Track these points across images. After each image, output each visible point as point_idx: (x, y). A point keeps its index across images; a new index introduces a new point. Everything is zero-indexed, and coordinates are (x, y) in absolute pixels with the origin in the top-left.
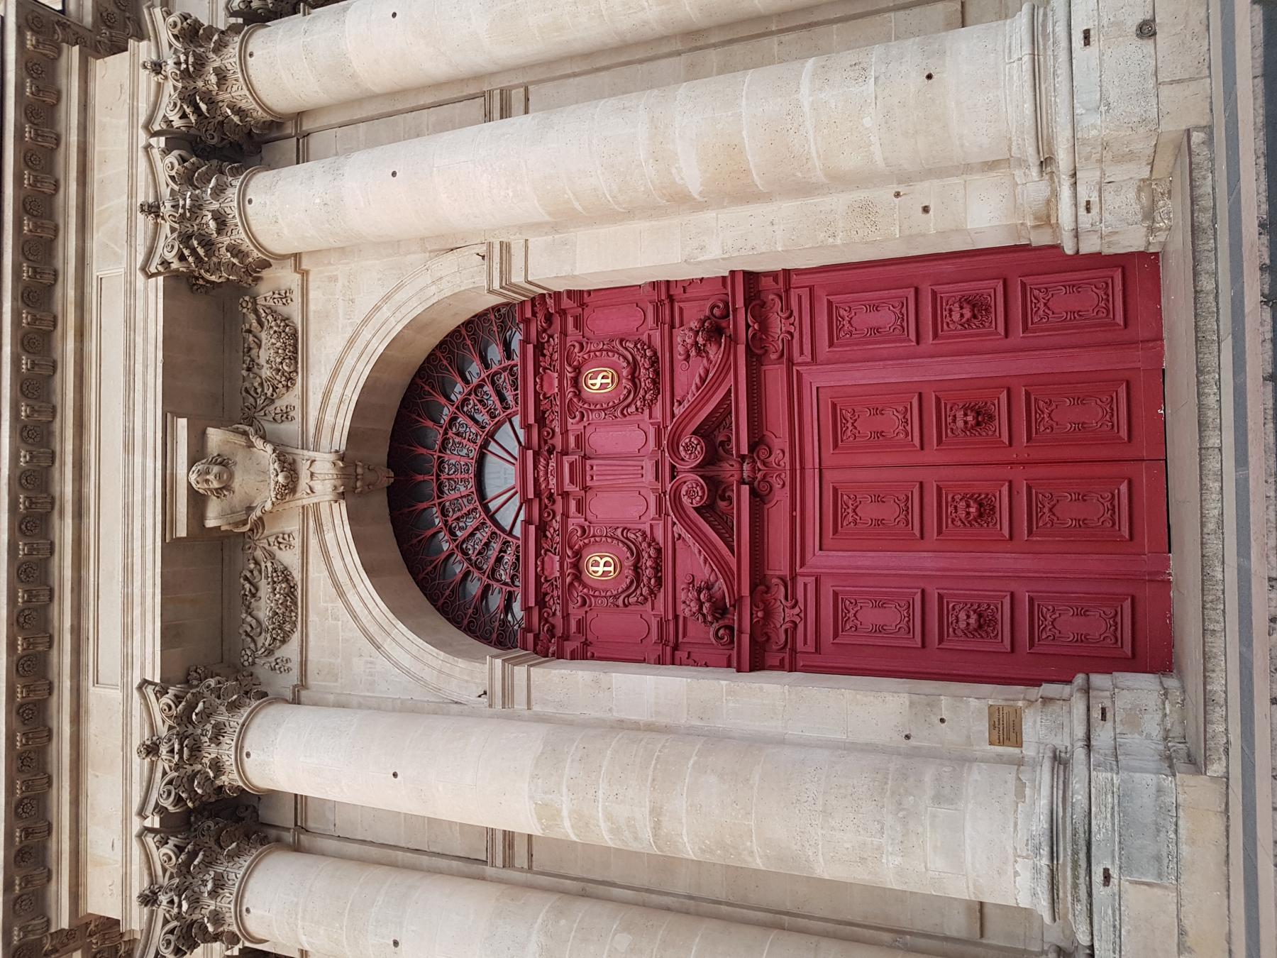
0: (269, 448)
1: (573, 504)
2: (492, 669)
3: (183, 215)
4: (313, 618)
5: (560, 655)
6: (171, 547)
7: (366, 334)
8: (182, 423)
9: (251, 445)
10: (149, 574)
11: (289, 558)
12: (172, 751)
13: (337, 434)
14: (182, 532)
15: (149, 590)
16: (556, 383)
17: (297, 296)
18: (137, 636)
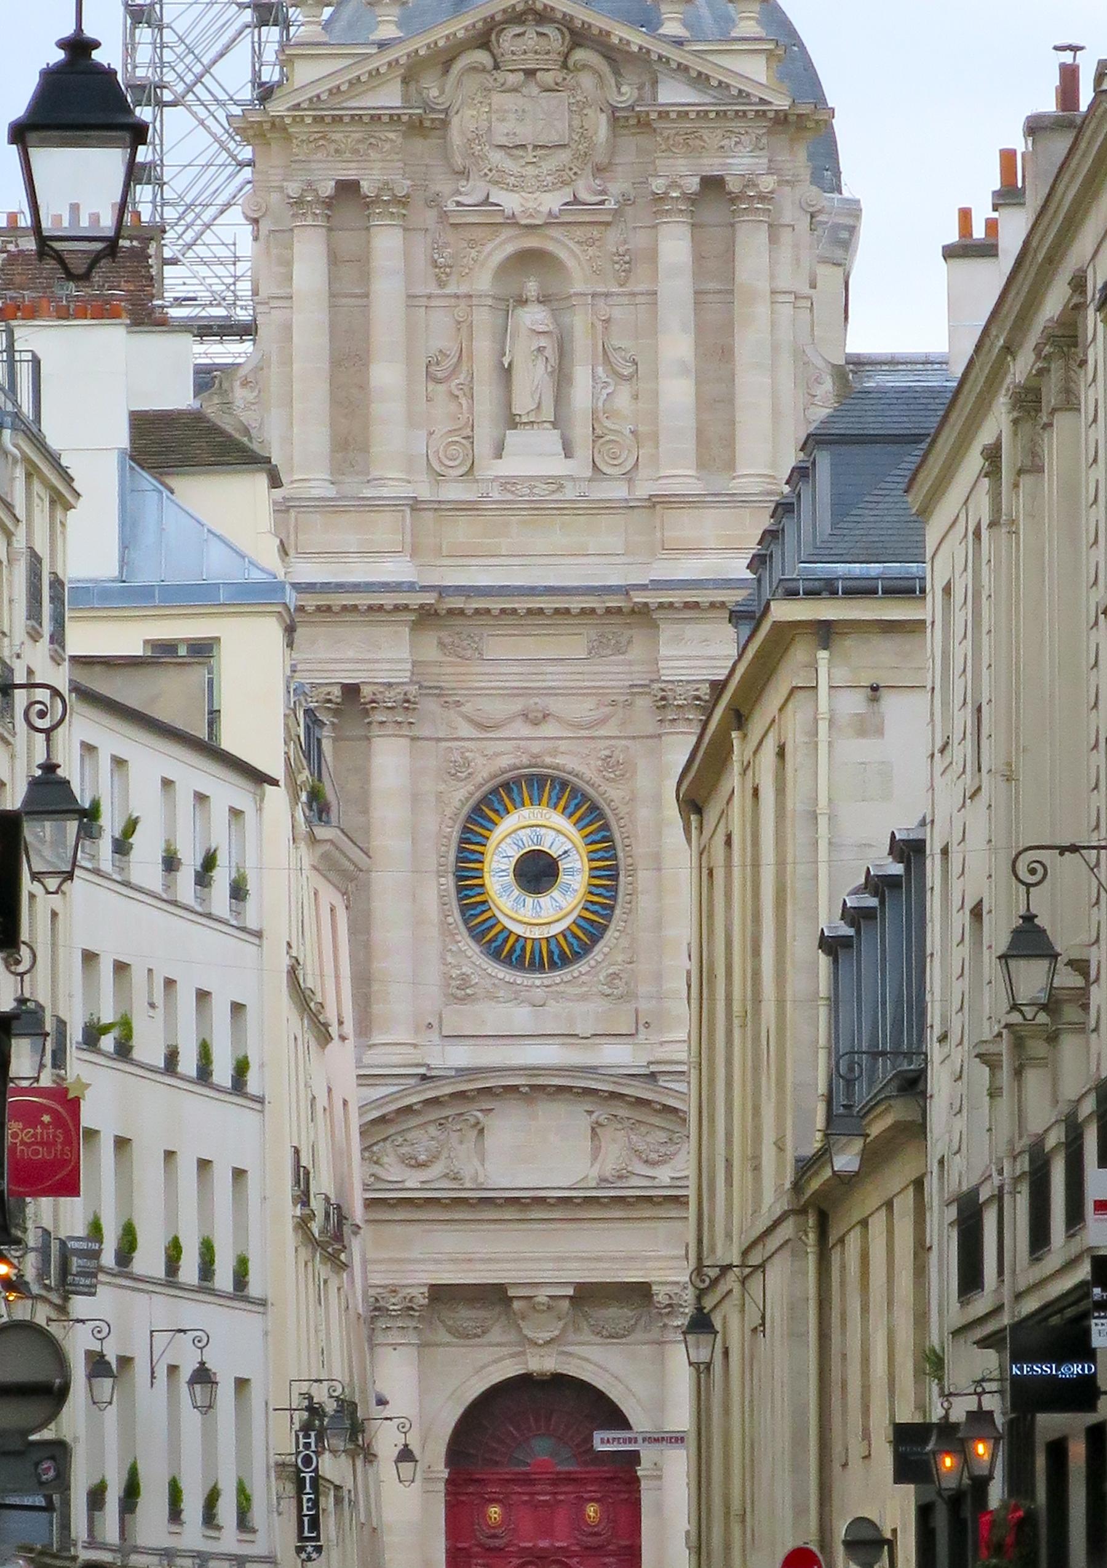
0: (557, 1333)
1: (526, 1498)
2: (441, 1472)
3: (681, 1306)
4: (463, 1350)
5: (448, 1493)
6: (501, 1288)
7: (621, 1387)
8: (571, 1292)
9: (560, 1319)
10: (487, 1274)
11: (496, 1334)
12: (394, 1304)
13: (567, 1367)
14: (511, 1293)
15: (477, 1274)
16: (592, 1489)
17: (647, 1336)
18: (451, 1267)
